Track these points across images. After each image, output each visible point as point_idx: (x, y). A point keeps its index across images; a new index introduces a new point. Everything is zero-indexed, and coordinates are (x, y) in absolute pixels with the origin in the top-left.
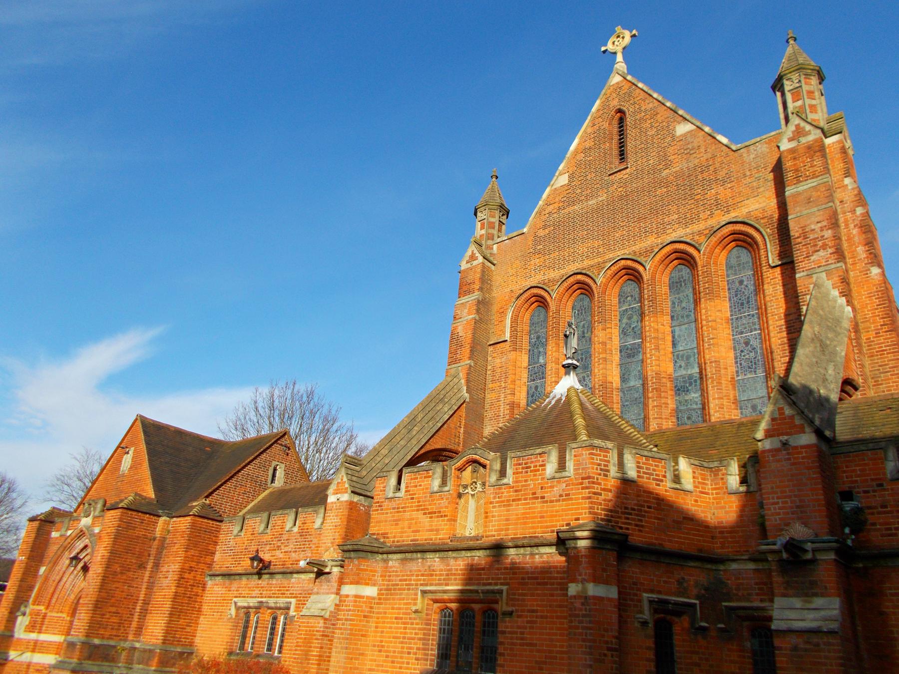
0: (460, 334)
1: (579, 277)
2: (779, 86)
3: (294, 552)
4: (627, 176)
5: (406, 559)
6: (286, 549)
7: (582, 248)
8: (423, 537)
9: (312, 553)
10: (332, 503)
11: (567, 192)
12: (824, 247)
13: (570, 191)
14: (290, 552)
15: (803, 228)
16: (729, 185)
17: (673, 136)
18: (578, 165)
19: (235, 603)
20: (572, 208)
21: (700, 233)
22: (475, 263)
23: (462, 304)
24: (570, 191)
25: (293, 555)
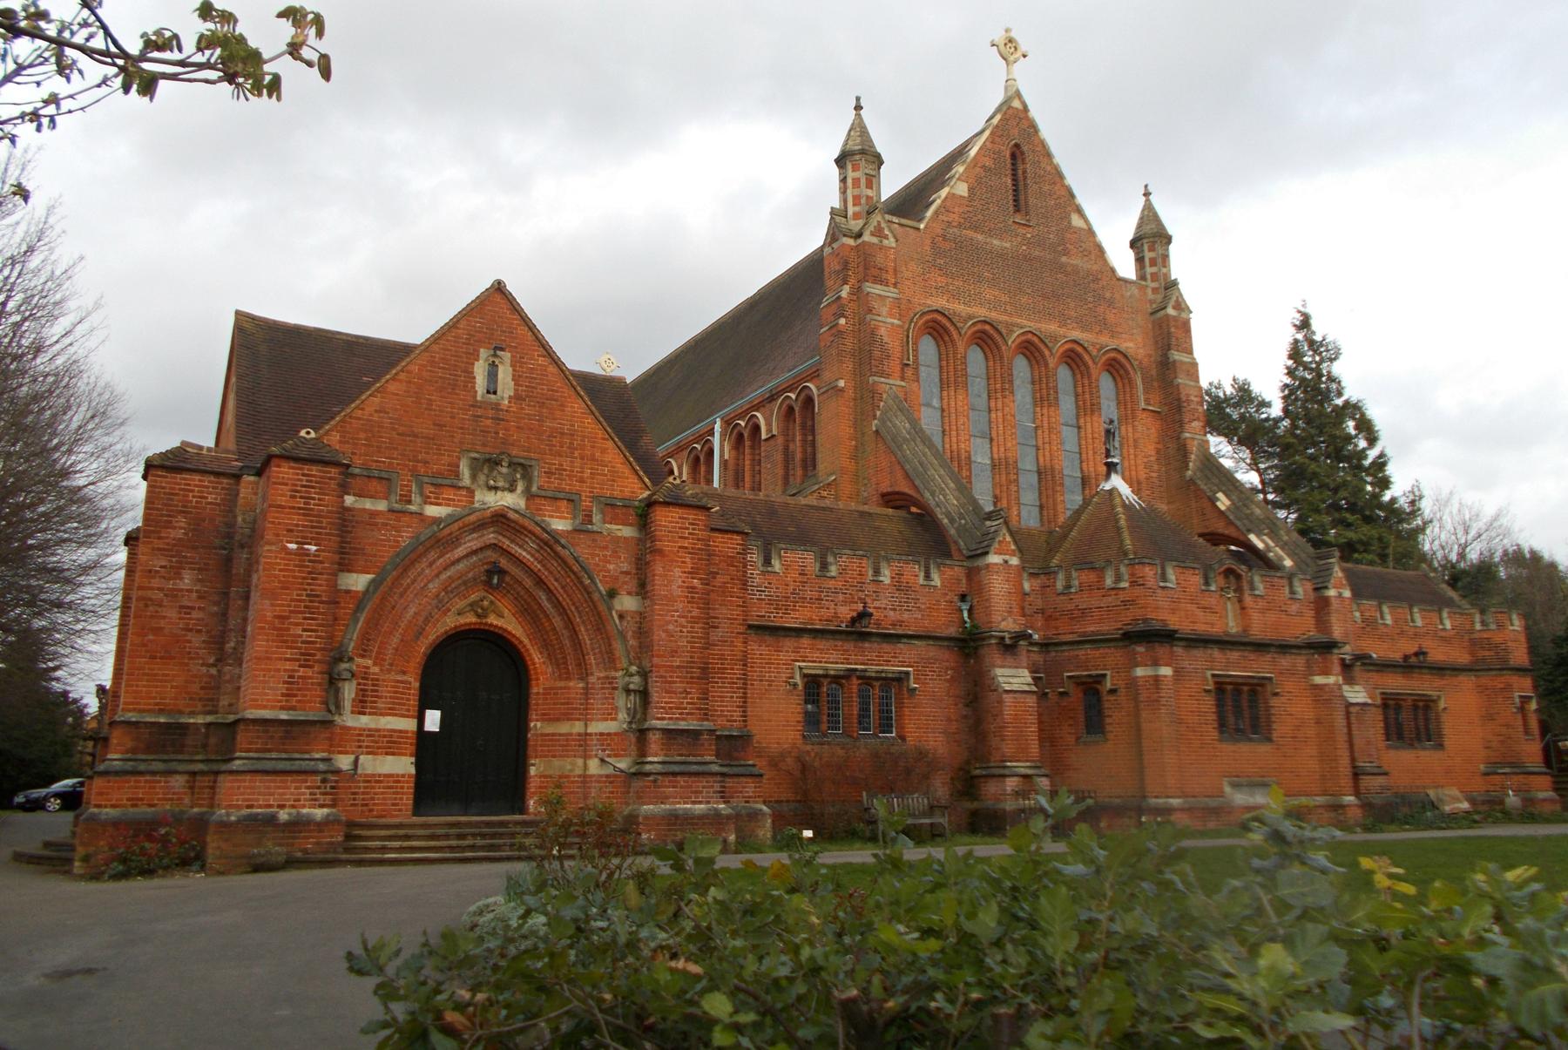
0: (886, 339)
1: (987, 327)
2: (1151, 240)
3: (891, 609)
4: (1029, 236)
5: (1190, 646)
6: (877, 604)
7: (989, 293)
8: (1201, 628)
9: (923, 615)
10: (996, 564)
11: (968, 209)
12: (1198, 419)
13: (971, 209)
14: (885, 609)
15: (1188, 395)
16: (1114, 311)
17: (1069, 222)
18: (979, 180)
19: (800, 668)
20: (975, 235)
21: (1093, 345)
22: (885, 242)
23: (880, 295)
24: (971, 209)
25: (892, 613)
